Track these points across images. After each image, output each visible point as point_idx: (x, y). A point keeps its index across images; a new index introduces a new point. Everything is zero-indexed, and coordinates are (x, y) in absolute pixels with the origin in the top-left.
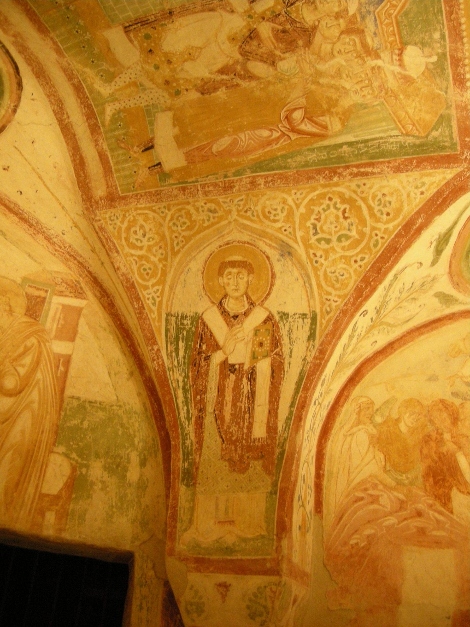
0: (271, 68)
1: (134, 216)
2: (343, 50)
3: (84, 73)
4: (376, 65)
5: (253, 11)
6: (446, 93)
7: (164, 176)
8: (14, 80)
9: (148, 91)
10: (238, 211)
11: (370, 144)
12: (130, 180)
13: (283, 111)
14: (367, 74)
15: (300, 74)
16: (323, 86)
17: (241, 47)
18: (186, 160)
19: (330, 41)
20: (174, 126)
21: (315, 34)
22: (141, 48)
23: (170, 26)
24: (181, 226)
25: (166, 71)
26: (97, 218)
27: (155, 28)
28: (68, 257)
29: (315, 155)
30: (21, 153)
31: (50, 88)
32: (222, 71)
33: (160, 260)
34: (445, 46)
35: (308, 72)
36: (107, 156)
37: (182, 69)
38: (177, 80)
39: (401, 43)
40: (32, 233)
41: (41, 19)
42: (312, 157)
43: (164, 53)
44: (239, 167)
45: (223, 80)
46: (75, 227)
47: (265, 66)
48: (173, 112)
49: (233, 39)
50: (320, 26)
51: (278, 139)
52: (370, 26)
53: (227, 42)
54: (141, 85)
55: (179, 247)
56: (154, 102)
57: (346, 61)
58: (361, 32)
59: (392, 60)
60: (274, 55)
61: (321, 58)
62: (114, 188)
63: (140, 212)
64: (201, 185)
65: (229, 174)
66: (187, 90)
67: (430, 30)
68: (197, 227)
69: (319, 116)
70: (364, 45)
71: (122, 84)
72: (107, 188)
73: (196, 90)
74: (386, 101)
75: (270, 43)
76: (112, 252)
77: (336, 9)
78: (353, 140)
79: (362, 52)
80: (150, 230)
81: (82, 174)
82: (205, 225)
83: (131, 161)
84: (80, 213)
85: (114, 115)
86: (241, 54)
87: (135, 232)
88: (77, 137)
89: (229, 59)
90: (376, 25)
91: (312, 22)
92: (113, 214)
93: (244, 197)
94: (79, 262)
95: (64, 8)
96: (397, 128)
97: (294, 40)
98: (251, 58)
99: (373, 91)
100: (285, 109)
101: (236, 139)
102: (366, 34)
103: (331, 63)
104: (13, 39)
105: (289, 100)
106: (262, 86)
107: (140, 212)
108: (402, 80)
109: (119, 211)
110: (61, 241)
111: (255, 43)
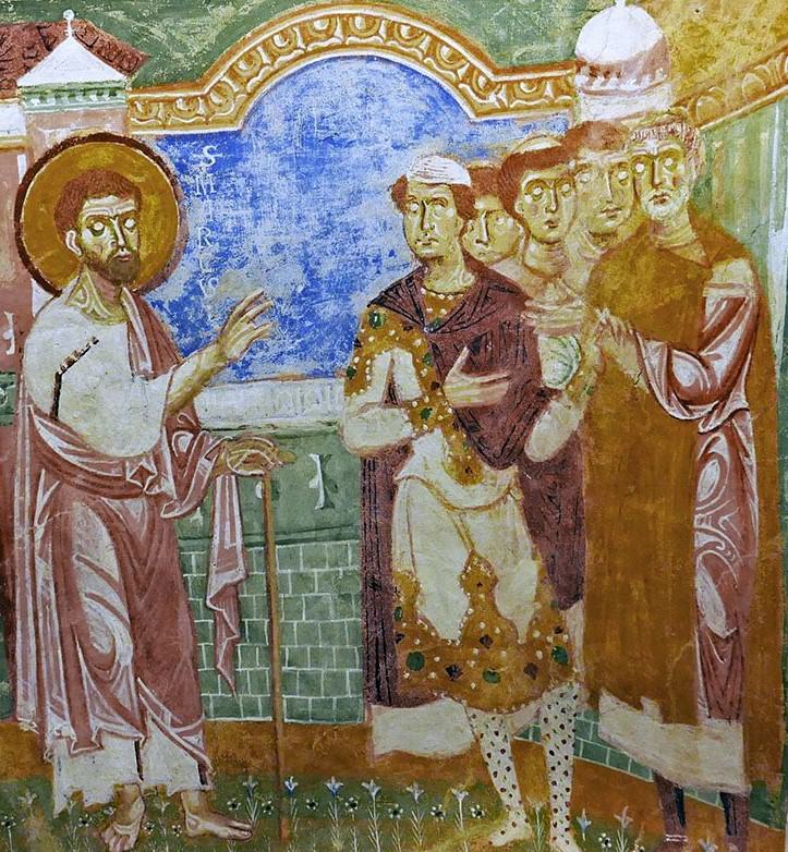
0: (553, 404)
2: (549, 216)
5: (415, 404)
9: (542, 725)
13: (666, 407)
14: (620, 164)
18: (729, 720)
20: (639, 706)
27: (400, 637)
35: (580, 315)
38: (532, 645)
49: (466, 474)
51: (734, 442)
59: (601, 93)
66: (559, 631)
71: (512, 777)
73: (564, 608)
74: (706, 122)
77: (451, 212)
79: (564, 168)
86: (505, 466)
99: (668, 154)
100: (663, 401)
105: (642, 383)
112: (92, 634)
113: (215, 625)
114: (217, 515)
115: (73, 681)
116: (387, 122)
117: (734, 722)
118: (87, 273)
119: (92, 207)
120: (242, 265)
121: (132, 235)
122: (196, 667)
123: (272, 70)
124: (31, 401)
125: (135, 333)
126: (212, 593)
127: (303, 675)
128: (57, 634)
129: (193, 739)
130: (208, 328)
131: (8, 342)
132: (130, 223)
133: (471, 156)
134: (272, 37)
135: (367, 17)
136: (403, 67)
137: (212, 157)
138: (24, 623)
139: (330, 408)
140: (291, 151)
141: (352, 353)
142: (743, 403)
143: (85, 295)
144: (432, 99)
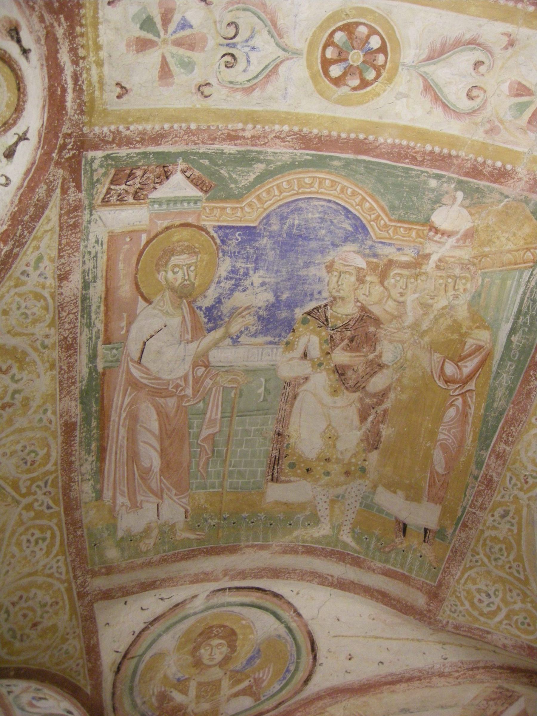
0: (385, 371)
1: (464, 590)
2: (401, 290)
3: (297, 537)
4: (436, 263)
5: (316, 360)
6: (507, 197)
7: (441, 533)
8: (268, 597)
9: (347, 495)
10: (521, 489)
11: (524, 309)
12: (426, 566)
13: (437, 381)
14: (440, 276)
15: (405, 345)
16: (430, 329)
17: (347, 388)
18: (436, 504)
19: (386, 299)
20: (395, 492)
21: (370, 311)
22: (299, 476)
23: (292, 441)
24: (502, 555)
25: (335, 468)
26: (444, 622)
28: (471, 673)
29: (505, 375)
30: (343, 636)
31: (295, 573)
32: (363, 418)
33: (523, 601)
34: (450, 178)
36: (389, 569)
37: (342, 453)
38: (350, 463)
39: (423, 225)
40: (426, 684)
41: (223, 545)
42: (505, 379)
43: (316, 460)
44: (474, 459)
45: (372, 422)
46: (444, 644)
47: (379, 375)
48: (380, 485)
50: (364, 302)
51: (465, 402)
52: (389, 252)
53: (336, 398)
54: (338, 497)
55: (522, 573)
56: (361, 496)
57: (415, 292)
58: (390, 263)
59: (439, 242)
60: (372, 361)
61: (399, 317)
62: (425, 585)
63: (462, 581)
64: (471, 507)
65: (476, 473)
66: (365, 460)
67: (424, 189)
68: (512, 541)
69: (463, 349)
70: (406, 266)
71: (328, 512)
72: (421, 591)
73: (369, 452)
74: (484, 269)
75: (356, 359)
76: (485, 637)
77: (353, 279)
78: (510, 325)
79: (414, 271)
80: (487, 586)
81: (395, 603)
82: (515, 531)
83: (407, 552)
84: (431, 631)
85: (353, 537)
86: (355, 392)
87: (480, 601)
88: (356, 582)
89: (353, 405)
90: (390, 244)
91: (355, 308)
92: (449, 606)
93: (509, 474)
94: (484, 668)
95: (222, 522)
96: (522, 271)
97: (366, 334)
98: (364, 385)
99: (464, 278)
100: (436, 379)
101: (441, 445)
102: (395, 259)
103: (409, 308)
104: (227, 578)
105: (428, 370)
106: (399, 389)
107: (462, 581)
108: (468, 241)
109: (450, 598)
110: (451, 666)
111: (350, 373)
112: (142, 459)
113: (200, 452)
114: (210, 405)
115: (131, 478)
116: (331, 232)
117: (438, 505)
118: (167, 293)
119: (175, 260)
120: (244, 291)
121: (192, 275)
122: (189, 470)
123: (279, 198)
124: (129, 355)
125: (185, 321)
126: (202, 438)
127: (239, 472)
128: (125, 460)
129: (184, 500)
130: (222, 320)
131: (123, 328)
132: (192, 268)
133: (369, 256)
134: (282, 183)
135: (332, 181)
136: (345, 208)
137: (239, 238)
138: (110, 457)
139: (274, 358)
140: (280, 239)
141: (291, 334)
142: (473, 388)
143: (164, 303)
144: (356, 226)
